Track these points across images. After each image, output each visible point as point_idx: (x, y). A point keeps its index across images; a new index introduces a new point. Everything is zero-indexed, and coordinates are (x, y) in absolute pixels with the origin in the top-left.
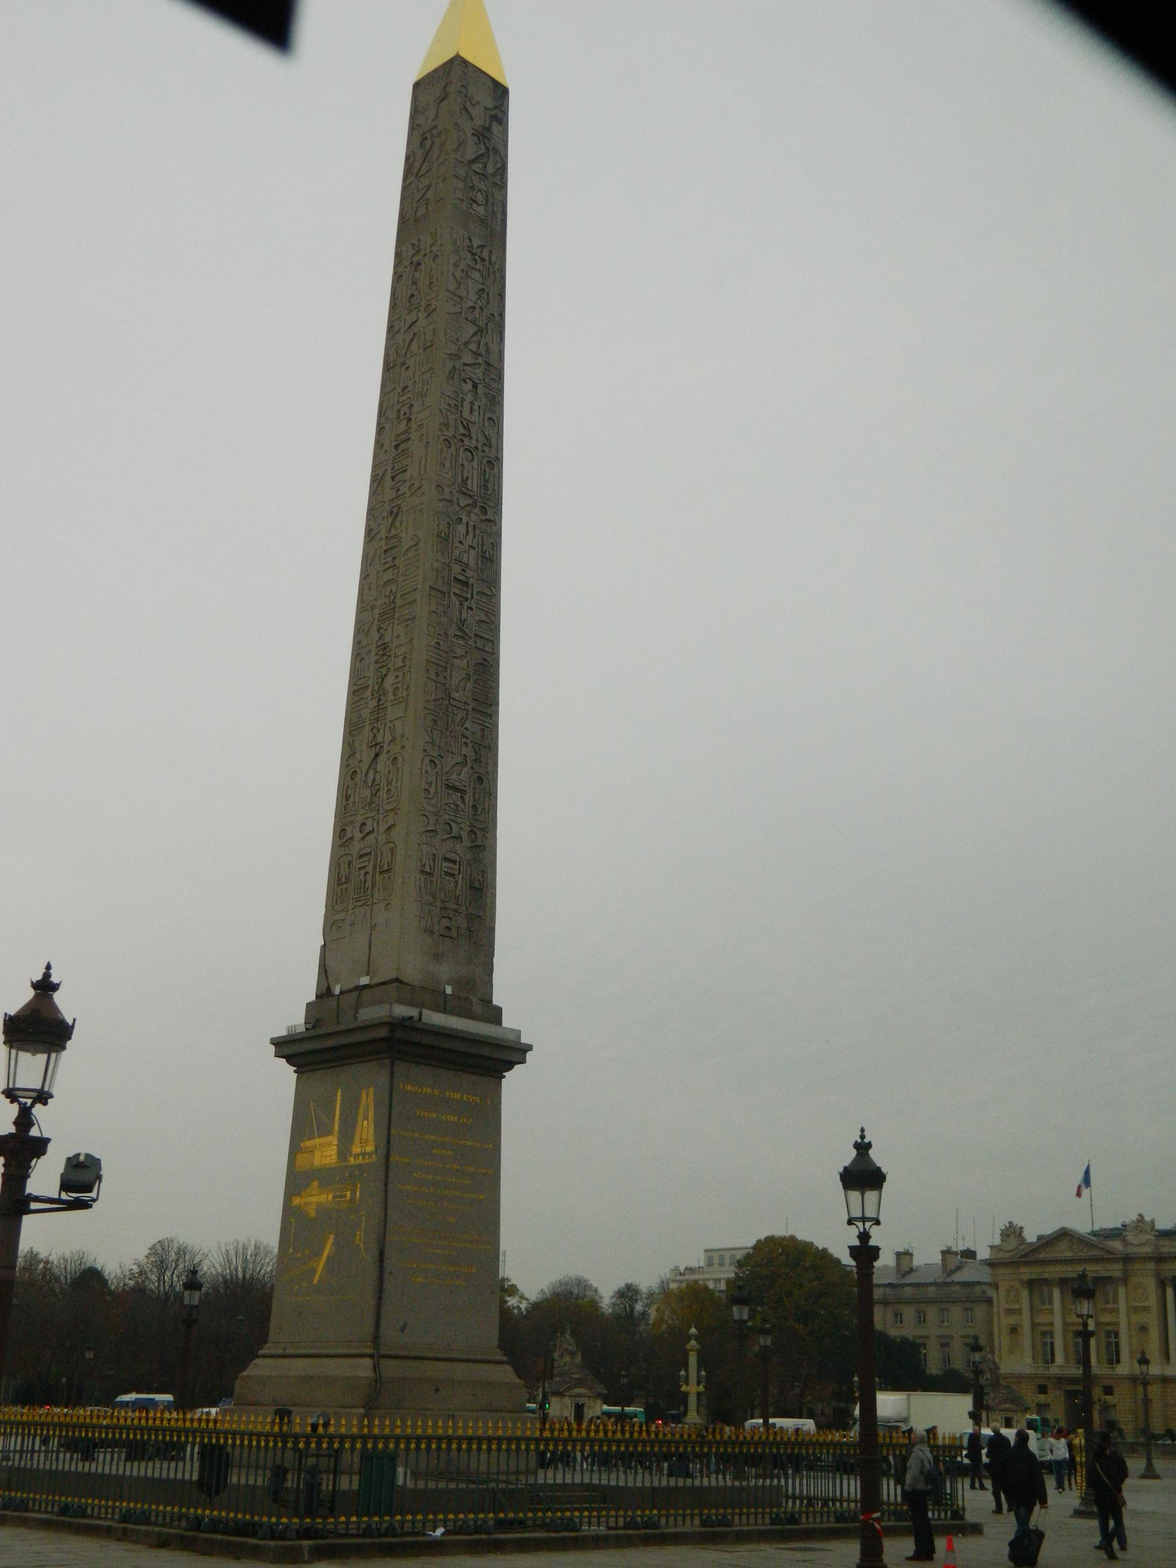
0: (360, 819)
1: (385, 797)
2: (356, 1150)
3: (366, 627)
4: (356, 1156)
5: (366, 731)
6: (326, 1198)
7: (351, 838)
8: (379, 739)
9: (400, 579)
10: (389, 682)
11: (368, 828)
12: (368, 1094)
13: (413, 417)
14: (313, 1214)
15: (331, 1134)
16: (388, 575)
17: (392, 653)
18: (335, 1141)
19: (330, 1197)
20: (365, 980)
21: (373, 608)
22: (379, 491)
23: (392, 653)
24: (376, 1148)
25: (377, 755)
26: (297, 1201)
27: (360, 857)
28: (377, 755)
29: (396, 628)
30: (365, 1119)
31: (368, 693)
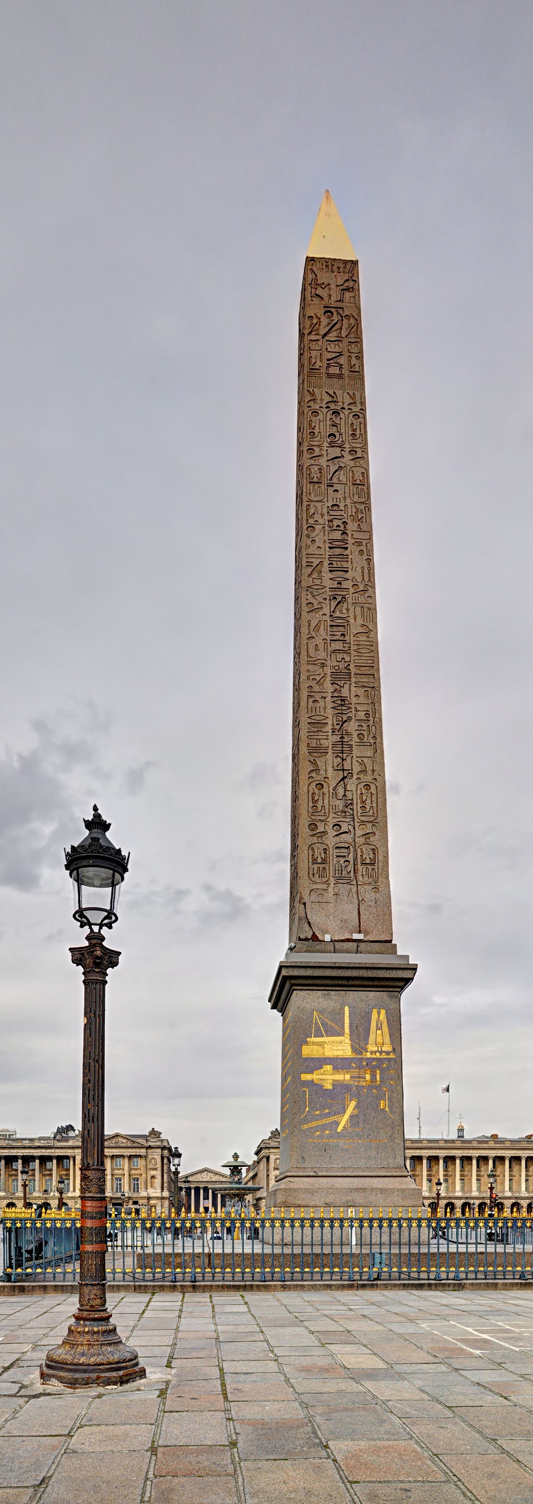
0: (332, 820)
1: (360, 811)
2: (372, 1047)
3: (318, 678)
4: (372, 1053)
5: (330, 756)
7: (325, 833)
9: (353, 653)
10: (352, 727)
11: (345, 828)
12: (379, 1014)
16: (338, 646)
17: (353, 706)
18: (348, 1041)
19: (348, 1077)
20: (356, 936)
21: (323, 665)
22: (315, 575)
24: (394, 1050)
29: (353, 689)
30: (378, 1028)
31: (329, 728)
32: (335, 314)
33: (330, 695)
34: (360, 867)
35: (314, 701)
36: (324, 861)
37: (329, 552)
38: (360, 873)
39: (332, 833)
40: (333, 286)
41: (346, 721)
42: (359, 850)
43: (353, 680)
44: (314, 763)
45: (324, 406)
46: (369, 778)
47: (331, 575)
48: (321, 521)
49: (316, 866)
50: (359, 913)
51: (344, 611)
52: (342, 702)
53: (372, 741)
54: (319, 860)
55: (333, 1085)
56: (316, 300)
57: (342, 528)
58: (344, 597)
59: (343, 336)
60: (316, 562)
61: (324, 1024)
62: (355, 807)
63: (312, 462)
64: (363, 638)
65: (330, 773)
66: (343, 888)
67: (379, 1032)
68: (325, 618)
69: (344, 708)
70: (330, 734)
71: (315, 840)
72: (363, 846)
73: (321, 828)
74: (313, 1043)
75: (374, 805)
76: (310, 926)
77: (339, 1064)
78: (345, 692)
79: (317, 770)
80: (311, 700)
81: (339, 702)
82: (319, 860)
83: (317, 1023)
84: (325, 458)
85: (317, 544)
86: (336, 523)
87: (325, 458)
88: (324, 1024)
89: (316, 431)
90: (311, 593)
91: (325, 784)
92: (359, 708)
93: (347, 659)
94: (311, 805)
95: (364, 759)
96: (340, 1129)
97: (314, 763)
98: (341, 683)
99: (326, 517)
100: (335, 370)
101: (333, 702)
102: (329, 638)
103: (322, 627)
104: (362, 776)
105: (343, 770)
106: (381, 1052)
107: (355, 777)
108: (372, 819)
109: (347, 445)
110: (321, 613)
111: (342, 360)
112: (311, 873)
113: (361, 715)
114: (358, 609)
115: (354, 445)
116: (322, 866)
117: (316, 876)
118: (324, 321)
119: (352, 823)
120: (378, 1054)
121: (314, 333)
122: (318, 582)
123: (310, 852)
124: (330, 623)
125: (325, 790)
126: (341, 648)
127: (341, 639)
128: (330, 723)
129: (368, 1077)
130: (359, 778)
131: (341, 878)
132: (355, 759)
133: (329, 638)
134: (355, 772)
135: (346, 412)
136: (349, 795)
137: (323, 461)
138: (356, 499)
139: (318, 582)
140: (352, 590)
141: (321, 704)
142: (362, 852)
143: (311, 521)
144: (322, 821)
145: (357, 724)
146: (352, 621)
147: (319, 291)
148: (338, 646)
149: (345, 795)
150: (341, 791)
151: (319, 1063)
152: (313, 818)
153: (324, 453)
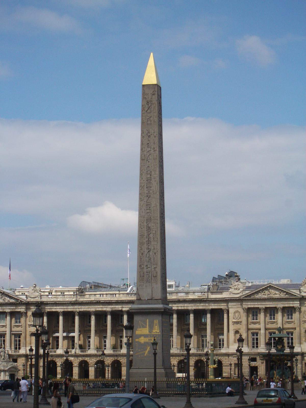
0: (145, 264)
1: (153, 261)
2: (154, 331)
3: (143, 221)
4: (154, 333)
6: (147, 340)
7: (143, 268)
9: (152, 213)
10: (151, 235)
11: (149, 266)
13: (152, 175)
14: (143, 343)
15: (145, 327)
16: (148, 211)
17: (152, 229)
18: (148, 329)
19: (148, 340)
21: (144, 217)
22: (142, 190)
23: (152, 229)
24: (160, 332)
25: (149, 251)
27: (147, 272)
29: (152, 224)
31: (145, 236)
32: (150, 103)
33: (146, 226)
34: (153, 278)
35: (142, 228)
36: (143, 276)
38: (153, 280)
39: (145, 268)
40: (149, 94)
41: (150, 234)
42: (152, 273)
43: (152, 221)
45: (146, 135)
46: (155, 251)
47: (146, 189)
49: (141, 278)
51: (150, 200)
53: (157, 239)
54: (142, 276)
55: (144, 342)
57: (150, 174)
58: (150, 196)
59: (152, 110)
65: (145, 250)
67: (156, 326)
68: (145, 202)
69: (149, 230)
70: (145, 238)
71: (141, 270)
73: (142, 267)
74: (140, 330)
77: (145, 336)
78: (150, 225)
79: (142, 249)
80: (141, 228)
81: (148, 228)
82: (142, 276)
85: (143, 179)
89: (144, 143)
90: (141, 195)
91: (144, 254)
92: (154, 230)
93: (150, 215)
94: (140, 260)
95: (154, 245)
96: (145, 355)
98: (149, 222)
100: (149, 122)
101: (146, 228)
102: (146, 209)
104: (154, 250)
105: (149, 249)
106: (156, 332)
107: (152, 251)
108: (156, 263)
109: (152, 147)
110: (144, 201)
111: (152, 119)
112: (140, 280)
113: (154, 232)
115: (154, 146)
116: (143, 278)
117: (141, 281)
118: (147, 106)
119: (151, 265)
121: (144, 110)
122: (143, 191)
124: (146, 204)
125: (144, 255)
126: (149, 212)
128: (145, 235)
130: (153, 251)
131: (147, 281)
132: (152, 245)
133: (146, 209)
134: (152, 249)
135: (152, 136)
136: (150, 256)
138: (154, 164)
139: (143, 191)
140: (152, 193)
142: (153, 273)
144: (143, 264)
145: (153, 235)
146: (152, 203)
148: (148, 211)
149: (149, 256)
150: (148, 255)
151: (140, 336)
152: (141, 264)
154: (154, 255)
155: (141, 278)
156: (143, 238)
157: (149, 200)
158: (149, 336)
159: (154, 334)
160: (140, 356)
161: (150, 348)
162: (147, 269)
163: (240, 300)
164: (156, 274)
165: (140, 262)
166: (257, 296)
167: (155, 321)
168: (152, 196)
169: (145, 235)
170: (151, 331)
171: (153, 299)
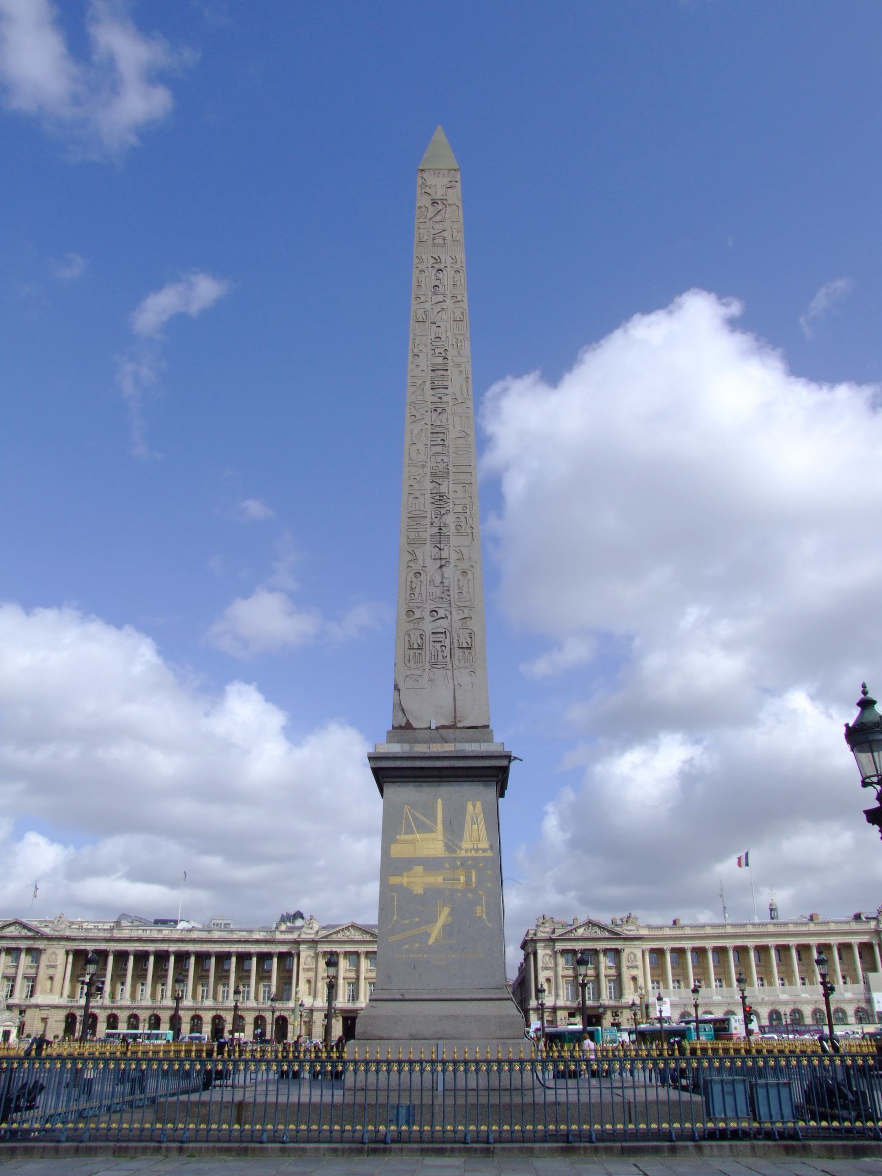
0: (430, 606)
1: (457, 596)
2: (466, 845)
6: (437, 880)
8: (444, 554)
9: (452, 455)
10: (450, 519)
11: (442, 613)
15: (431, 830)
16: (439, 449)
17: (450, 501)
18: (441, 837)
19: (440, 879)
23: (450, 501)
24: (491, 847)
25: (441, 567)
26: (394, 880)
28: (441, 567)
30: (473, 823)
31: (427, 521)
34: (456, 651)
36: (420, 648)
37: (431, 374)
38: (457, 657)
42: (456, 635)
43: (452, 477)
44: (412, 553)
45: (430, 266)
46: (465, 565)
47: (432, 392)
48: (424, 350)
49: (412, 652)
50: (454, 698)
51: (444, 420)
52: (440, 498)
53: (469, 531)
54: (416, 646)
55: (425, 889)
56: (425, 196)
57: (443, 354)
60: (419, 382)
61: (416, 820)
62: (451, 593)
63: (419, 307)
64: (462, 441)
65: (429, 562)
66: (439, 674)
67: (475, 827)
68: (426, 427)
71: (411, 626)
72: (461, 631)
73: (418, 614)
75: (471, 590)
76: (404, 713)
77: (431, 864)
78: (443, 489)
81: (438, 498)
83: (407, 818)
84: (430, 303)
86: (438, 351)
87: (430, 303)
88: (416, 820)
92: (457, 502)
94: (408, 592)
97: (412, 553)
99: (430, 347)
102: (429, 443)
103: (423, 435)
105: (441, 559)
106: (477, 850)
107: (452, 565)
111: (445, 234)
112: (407, 658)
113: (459, 509)
114: (457, 419)
116: (417, 652)
117: (412, 662)
118: (431, 209)
119: (448, 609)
120: (473, 851)
122: (421, 398)
123: (407, 638)
125: (423, 577)
127: (442, 443)
128: (429, 516)
129: (462, 879)
133: (429, 443)
135: (448, 269)
136: (446, 582)
137: (427, 306)
138: (456, 331)
139: (421, 398)
140: (451, 403)
141: (421, 500)
142: (459, 636)
143: (416, 351)
146: (451, 428)
147: (428, 190)
148: (439, 449)
150: (438, 580)
151: (408, 864)
153: (429, 300)
154: (460, 578)
155: (411, 654)
156: (419, 526)
157: (441, 421)
158: (447, 865)
159: (469, 855)
160: (407, 946)
161: (449, 914)
162: (434, 625)
163: (314, 943)
164: (469, 640)
165: (408, 598)
166: (334, 937)
167: (470, 807)
168: (449, 410)
169: (429, 516)
170: (451, 845)
171: (459, 725)
